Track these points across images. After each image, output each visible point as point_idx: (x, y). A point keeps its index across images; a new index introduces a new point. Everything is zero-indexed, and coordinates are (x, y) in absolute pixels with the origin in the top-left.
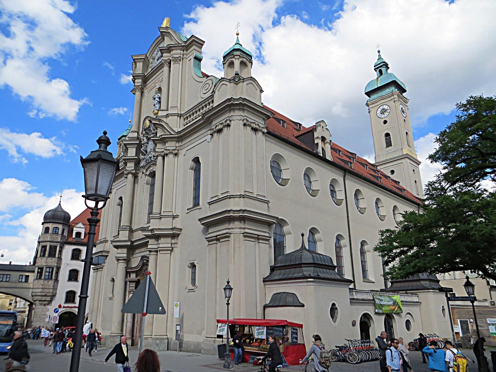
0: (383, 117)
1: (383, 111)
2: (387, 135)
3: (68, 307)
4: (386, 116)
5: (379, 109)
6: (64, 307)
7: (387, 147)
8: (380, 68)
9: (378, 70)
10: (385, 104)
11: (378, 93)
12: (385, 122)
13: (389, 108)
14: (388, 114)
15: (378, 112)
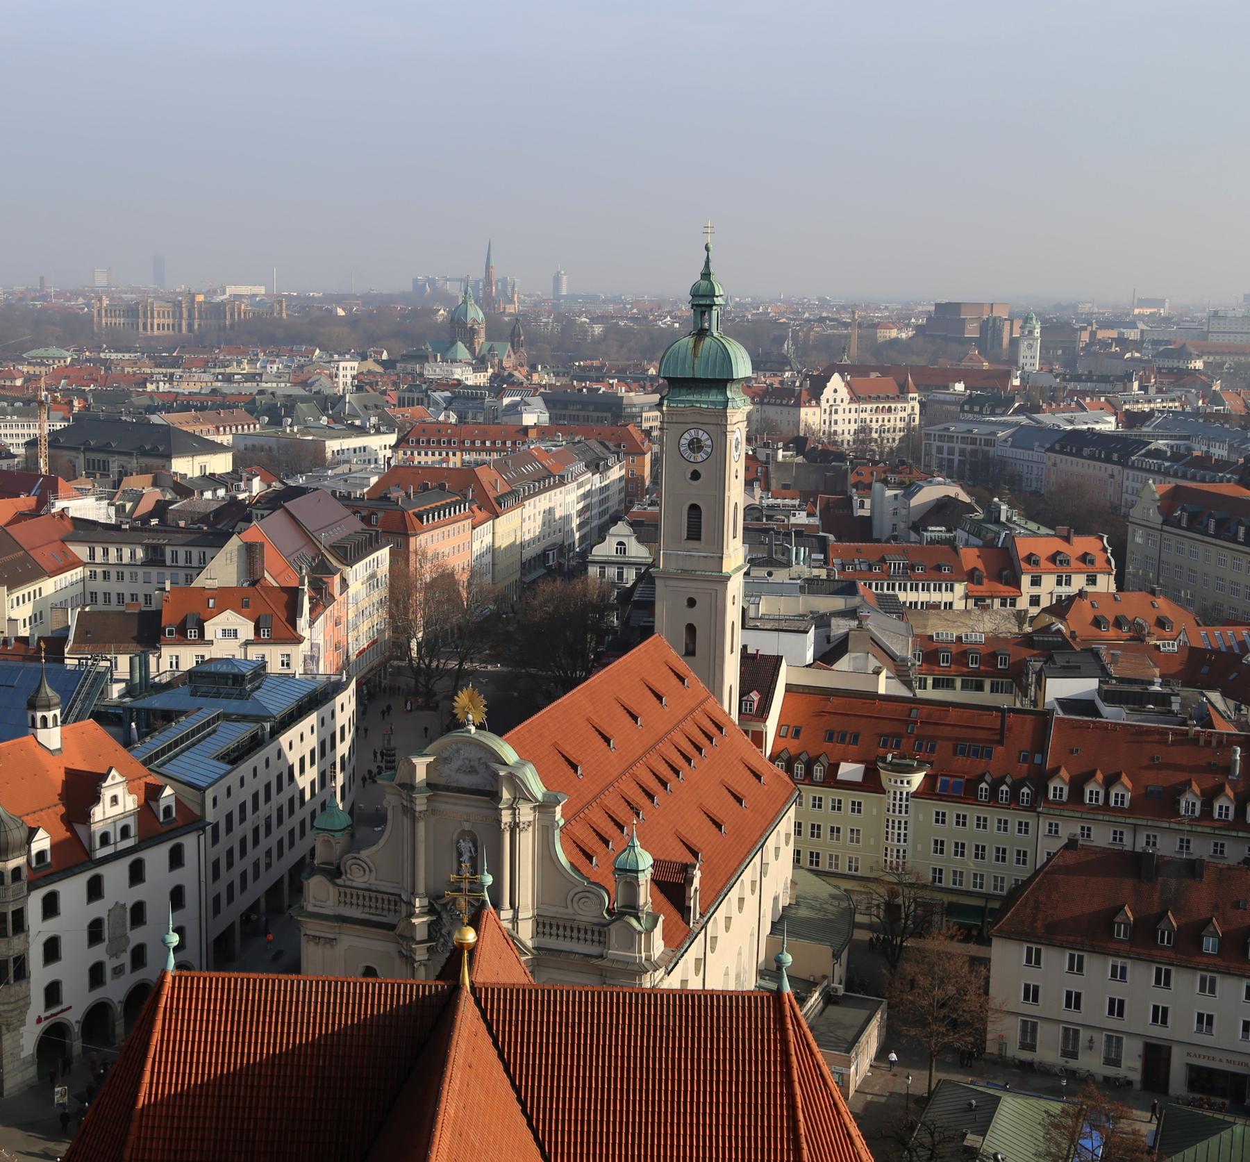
0: (692, 460)
1: (696, 445)
2: (694, 509)
3: (53, 1015)
4: (700, 459)
5: (686, 435)
6: (46, 1018)
7: (688, 538)
8: (704, 309)
9: (699, 309)
10: (704, 427)
11: (690, 388)
12: (695, 476)
13: (709, 442)
14: (705, 457)
15: (683, 441)
